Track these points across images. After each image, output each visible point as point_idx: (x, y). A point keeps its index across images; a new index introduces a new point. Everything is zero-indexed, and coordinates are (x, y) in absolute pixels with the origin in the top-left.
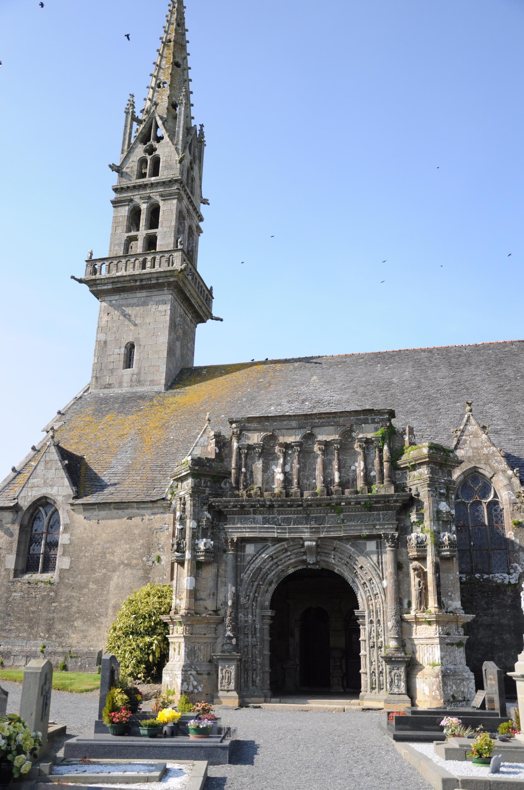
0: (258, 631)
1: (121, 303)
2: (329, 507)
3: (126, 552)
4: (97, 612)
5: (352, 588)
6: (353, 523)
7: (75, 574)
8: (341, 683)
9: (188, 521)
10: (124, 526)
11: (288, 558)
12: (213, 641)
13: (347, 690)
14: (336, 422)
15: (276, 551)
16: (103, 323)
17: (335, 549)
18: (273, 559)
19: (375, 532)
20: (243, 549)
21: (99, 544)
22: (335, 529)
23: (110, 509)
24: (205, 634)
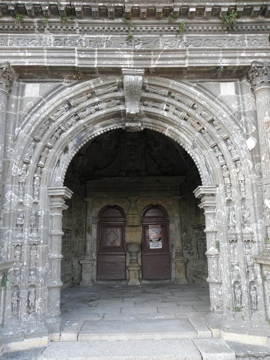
0: (41, 221)
8: (137, 276)
11: (96, 107)
13: (143, 282)
15: (76, 93)
17: (170, 93)
18: (70, 107)
19: (238, 63)
22: (176, 56)
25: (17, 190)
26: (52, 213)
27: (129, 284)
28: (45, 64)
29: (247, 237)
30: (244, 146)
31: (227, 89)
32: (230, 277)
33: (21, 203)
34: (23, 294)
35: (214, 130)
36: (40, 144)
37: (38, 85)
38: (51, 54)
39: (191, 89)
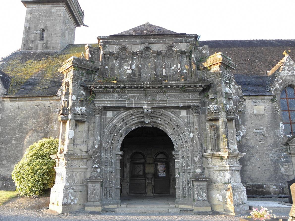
1: (38, 9)
2: (159, 89)
3: (34, 123)
4: (16, 156)
5: (170, 138)
6: (174, 99)
7: (3, 136)
8: (151, 191)
9: (70, 95)
10: (33, 110)
12: (85, 170)
14: (164, 41)
15: (126, 115)
16: (28, 18)
17: (161, 114)
18: (123, 120)
19: (187, 105)
20: (105, 114)
21: (18, 119)
22: (163, 102)
23: (26, 101)
27: (147, 195)
28: (115, 106)
29: (188, 171)
30: (189, 136)
31: (184, 113)
32: (182, 186)
33: (106, 157)
34: (108, 190)
35: (178, 129)
36: (113, 135)
37: (111, 112)
38: (117, 102)
39: (170, 114)
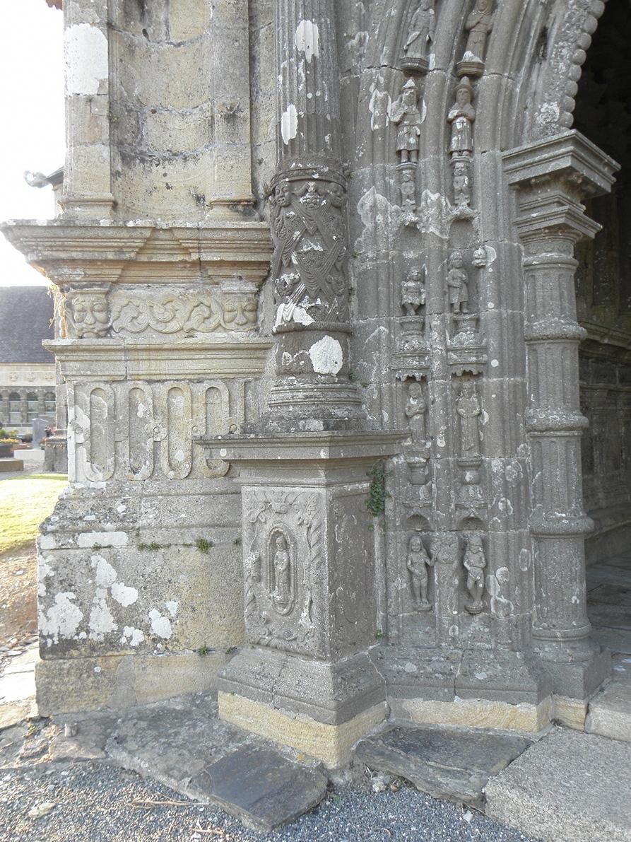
12: (242, 365)
24: (191, 333)
25: (392, 181)
26: (529, 254)
33: (412, 229)
34: (444, 544)
